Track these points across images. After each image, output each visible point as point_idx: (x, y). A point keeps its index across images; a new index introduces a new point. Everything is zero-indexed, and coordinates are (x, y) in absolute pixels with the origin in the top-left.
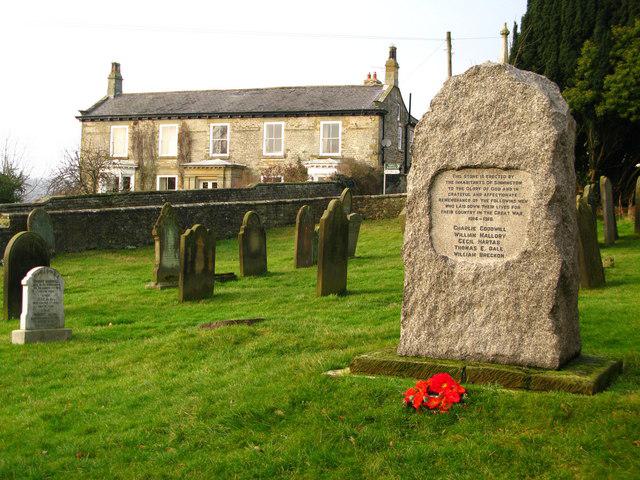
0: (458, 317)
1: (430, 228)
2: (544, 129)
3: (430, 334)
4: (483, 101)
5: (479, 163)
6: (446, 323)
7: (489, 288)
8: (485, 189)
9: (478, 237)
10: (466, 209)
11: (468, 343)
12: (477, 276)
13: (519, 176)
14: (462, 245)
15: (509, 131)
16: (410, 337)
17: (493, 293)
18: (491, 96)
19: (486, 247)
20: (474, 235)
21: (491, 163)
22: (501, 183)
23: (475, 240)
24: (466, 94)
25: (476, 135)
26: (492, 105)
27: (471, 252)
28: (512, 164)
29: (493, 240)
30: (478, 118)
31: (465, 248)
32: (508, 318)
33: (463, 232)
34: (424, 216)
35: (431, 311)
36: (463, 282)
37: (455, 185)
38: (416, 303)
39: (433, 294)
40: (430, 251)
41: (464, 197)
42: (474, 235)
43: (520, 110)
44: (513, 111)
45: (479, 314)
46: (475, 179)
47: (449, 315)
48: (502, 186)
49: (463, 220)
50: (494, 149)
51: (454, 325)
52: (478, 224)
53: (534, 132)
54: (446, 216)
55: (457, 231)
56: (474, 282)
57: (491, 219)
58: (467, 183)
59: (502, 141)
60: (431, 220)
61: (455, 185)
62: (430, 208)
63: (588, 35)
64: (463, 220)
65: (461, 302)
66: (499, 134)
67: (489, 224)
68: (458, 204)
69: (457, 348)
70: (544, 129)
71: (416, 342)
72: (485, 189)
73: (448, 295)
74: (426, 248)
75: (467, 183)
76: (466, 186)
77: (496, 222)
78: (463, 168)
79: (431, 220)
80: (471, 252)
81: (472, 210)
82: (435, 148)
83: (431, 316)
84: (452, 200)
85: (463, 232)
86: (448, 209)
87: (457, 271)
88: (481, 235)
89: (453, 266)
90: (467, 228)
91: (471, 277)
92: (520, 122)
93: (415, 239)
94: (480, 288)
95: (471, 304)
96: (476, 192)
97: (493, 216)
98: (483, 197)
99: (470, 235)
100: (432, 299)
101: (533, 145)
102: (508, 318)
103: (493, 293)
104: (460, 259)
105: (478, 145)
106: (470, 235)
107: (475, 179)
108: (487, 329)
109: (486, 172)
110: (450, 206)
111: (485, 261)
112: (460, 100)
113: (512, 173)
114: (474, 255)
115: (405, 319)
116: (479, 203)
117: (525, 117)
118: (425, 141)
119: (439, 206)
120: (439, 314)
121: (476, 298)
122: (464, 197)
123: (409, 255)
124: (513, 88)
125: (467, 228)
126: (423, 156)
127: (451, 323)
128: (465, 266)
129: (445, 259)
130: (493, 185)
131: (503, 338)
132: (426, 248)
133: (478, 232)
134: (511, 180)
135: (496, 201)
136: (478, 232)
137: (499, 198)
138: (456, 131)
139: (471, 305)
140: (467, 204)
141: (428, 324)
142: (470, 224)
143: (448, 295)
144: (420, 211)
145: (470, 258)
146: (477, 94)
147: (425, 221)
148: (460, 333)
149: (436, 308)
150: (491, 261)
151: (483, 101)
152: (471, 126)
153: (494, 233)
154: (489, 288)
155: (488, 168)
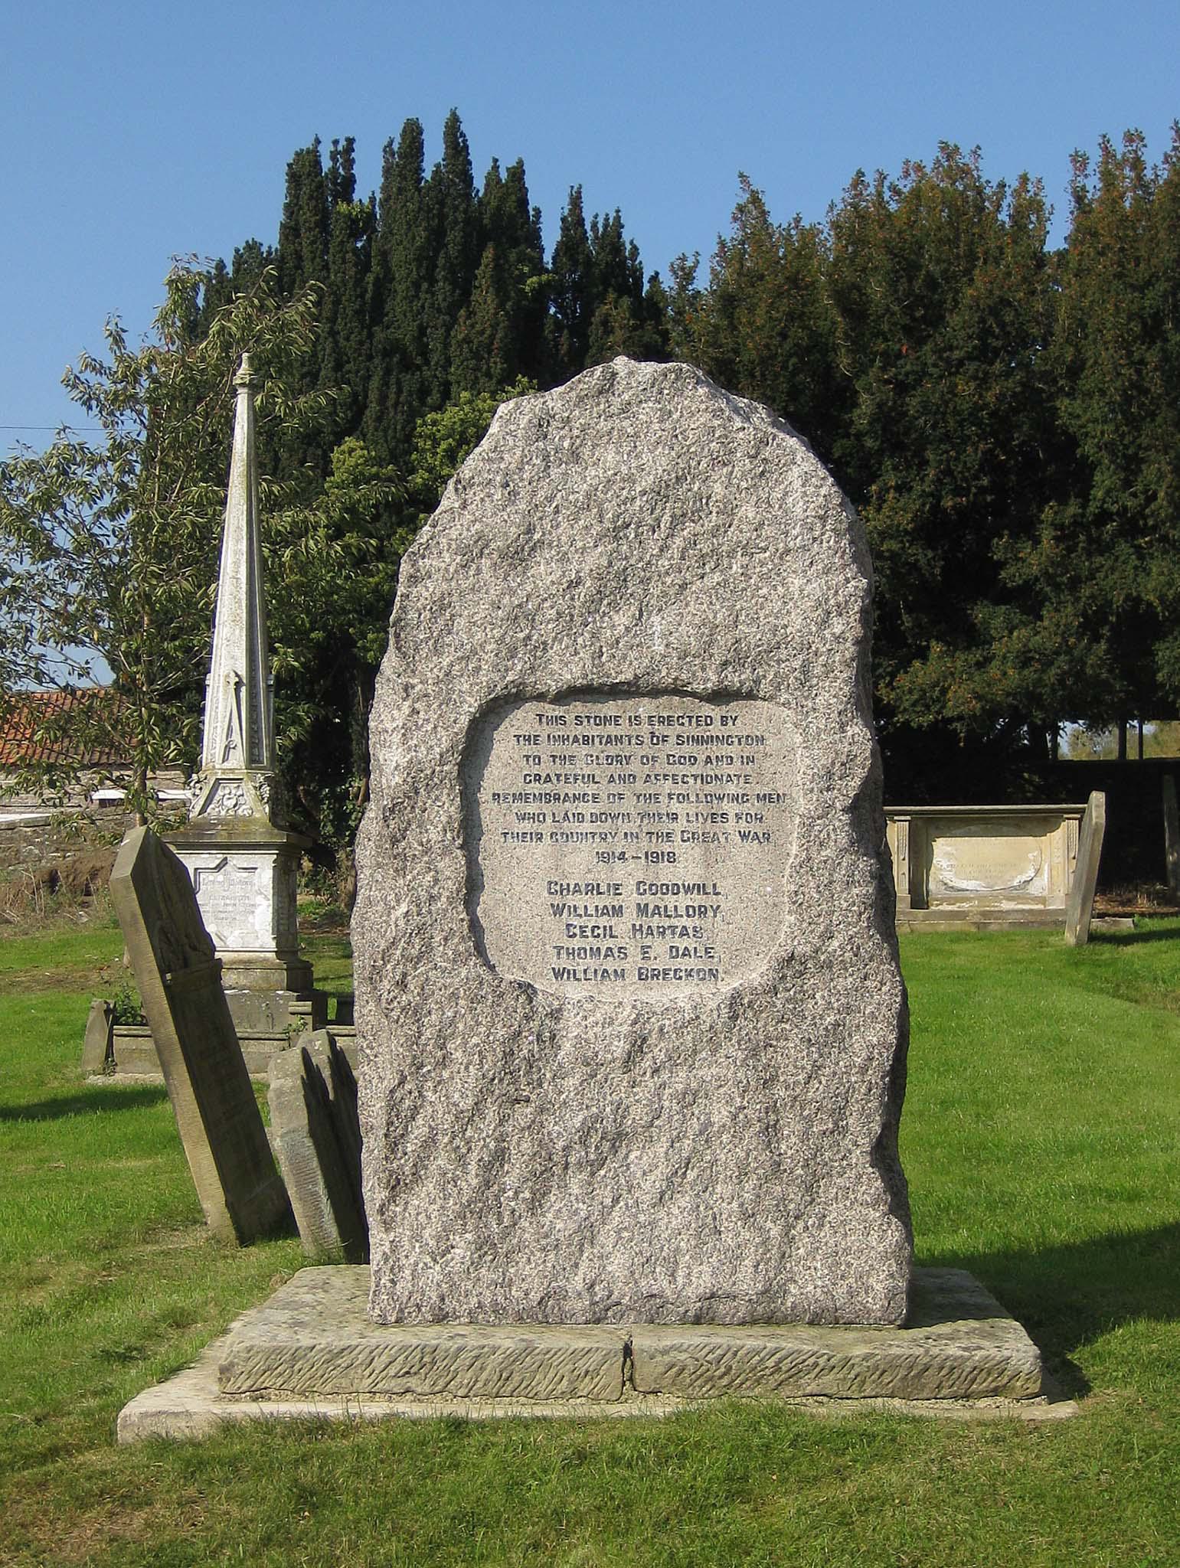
0: (575, 1184)
1: (473, 885)
2: (827, 571)
3: (484, 1246)
4: (630, 479)
5: (627, 676)
6: (535, 1204)
7: (680, 1080)
8: (645, 759)
9: (630, 917)
10: (587, 827)
11: (617, 1265)
12: (639, 1045)
13: (749, 717)
14: (576, 943)
15: (717, 577)
16: (412, 1256)
17: (688, 1098)
18: (657, 464)
19: (659, 947)
20: (618, 911)
21: (665, 676)
22: (698, 740)
23: (622, 926)
24: (575, 456)
25: (613, 586)
26: (660, 493)
27: (610, 965)
28: (733, 679)
29: (679, 919)
30: (616, 533)
31: (591, 952)
32: (743, 1173)
33: (579, 900)
34: (446, 852)
35: (487, 1167)
36: (591, 1064)
37: (544, 750)
38: (430, 1142)
39: (491, 1112)
40: (472, 968)
41: (579, 788)
42: (618, 911)
43: (748, 511)
44: (728, 511)
45: (647, 1164)
46: (611, 730)
47: (544, 1176)
48: (701, 752)
49: (579, 862)
50: (661, 635)
51: (560, 1215)
52: (628, 874)
53: (796, 582)
54: (521, 850)
55: (557, 900)
56: (629, 1062)
57: (672, 858)
58: (586, 740)
59: (695, 608)
60: (472, 864)
61: (544, 750)
62: (469, 829)
63: (352, 427)
64: (579, 862)
65: (586, 1132)
66: (683, 586)
67: (666, 873)
68: (560, 808)
69: (578, 1283)
70: (827, 571)
71: (435, 1273)
72: (645, 759)
73: (542, 1110)
74: (457, 959)
75: (586, 740)
76: (585, 750)
77: (688, 867)
78: (568, 695)
79: (472, 864)
80: (610, 965)
81: (606, 827)
82: (477, 623)
83: (487, 1184)
84: (547, 791)
85: (572, 900)
86: (527, 826)
87: (571, 1027)
88: (642, 910)
89: (555, 1015)
90: (594, 889)
91: (620, 1048)
92: (747, 549)
93: (420, 929)
94: (651, 1083)
95: (620, 1135)
96: (616, 769)
97: (677, 846)
98: (639, 786)
99: (605, 911)
100: (488, 1124)
101: (796, 622)
102: (743, 1173)
103: (688, 1098)
104: (574, 991)
105: (622, 619)
106: (605, 911)
107: (611, 730)
108: (677, 1214)
109: (645, 707)
110: (533, 817)
111: (659, 995)
112: (555, 472)
113: (734, 708)
114: (620, 974)
115: (392, 1199)
116: (629, 805)
117: (767, 531)
118: (441, 605)
119: (490, 814)
120: (512, 1176)
121: (638, 1114)
122: (579, 788)
123: (402, 984)
124: (725, 441)
125: (594, 889)
126: (437, 651)
127: (554, 1200)
128: (594, 1011)
129: (527, 990)
130: (671, 747)
131: (728, 1239)
132: (457, 959)
133: (630, 898)
134: (730, 729)
135: (683, 798)
136: (630, 898)
137: (693, 787)
138: (544, 572)
139: (618, 1139)
140: (587, 808)
141: (481, 1206)
142: (602, 875)
143: (542, 1110)
144: (434, 835)
145: (607, 987)
146: (610, 457)
147: (452, 867)
148: (587, 1233)
149: (500, 1156)
150: (681, 994)
151: (630, 479)
152: (596, 558)
153: (683, 901)
154: (680, 1080)
155: (655, 692)
